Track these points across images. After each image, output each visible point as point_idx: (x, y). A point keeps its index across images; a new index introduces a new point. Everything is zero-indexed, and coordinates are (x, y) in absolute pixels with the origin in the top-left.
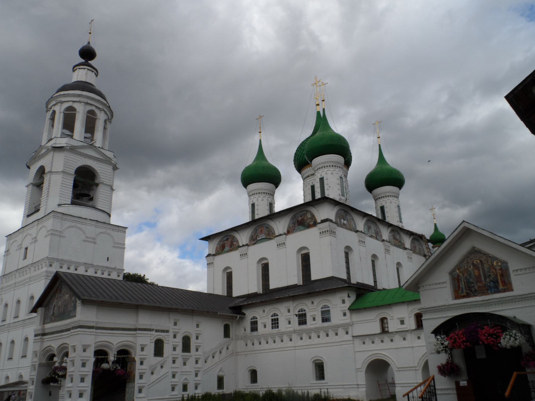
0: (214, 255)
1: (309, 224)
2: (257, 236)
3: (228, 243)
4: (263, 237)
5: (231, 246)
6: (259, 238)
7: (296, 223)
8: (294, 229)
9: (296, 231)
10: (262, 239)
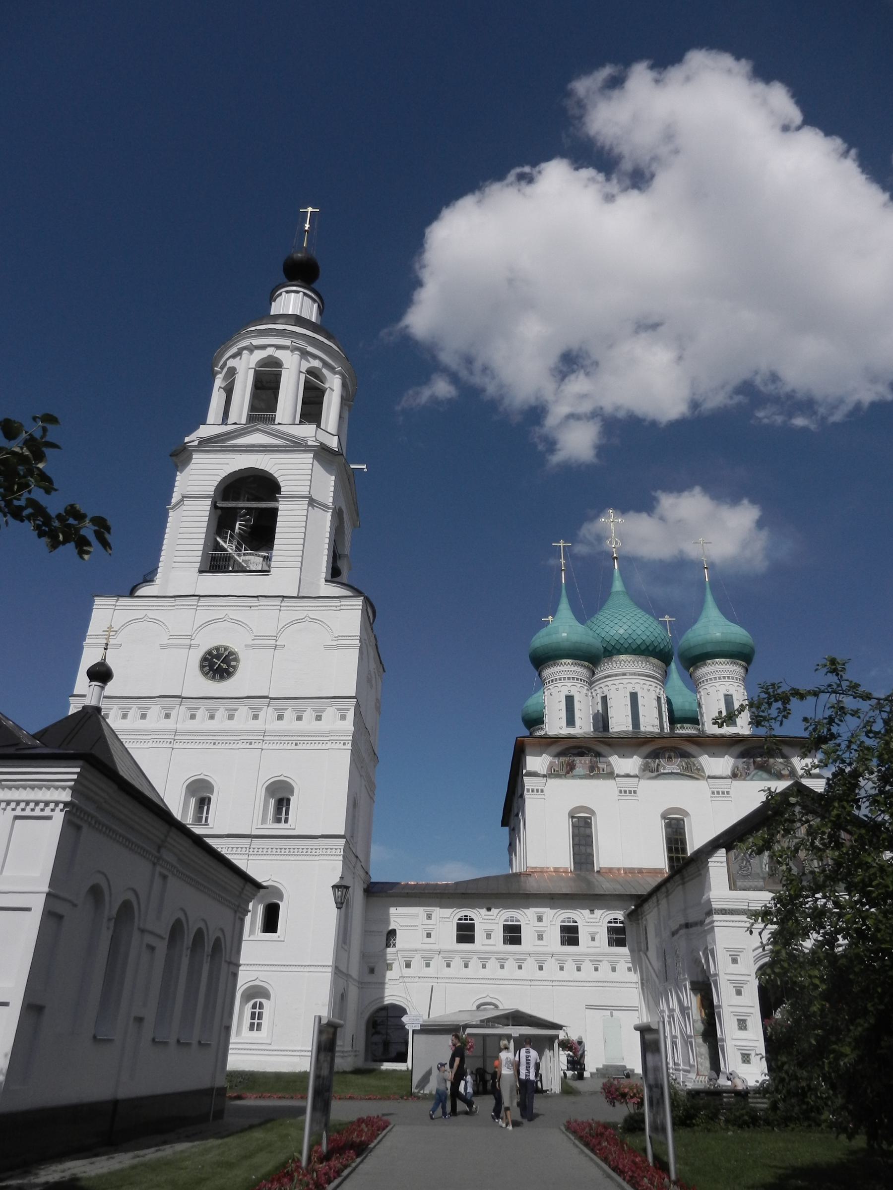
0: (544, 776)
1: (781, 773)
2: (658, 765)
3: (583, 762)
4: (675, 771)
5: (592, 769)
6: (664, 769)
7: (752, 764)
8: (748, 774)
9: (753, 776)
10: (672, 773)
